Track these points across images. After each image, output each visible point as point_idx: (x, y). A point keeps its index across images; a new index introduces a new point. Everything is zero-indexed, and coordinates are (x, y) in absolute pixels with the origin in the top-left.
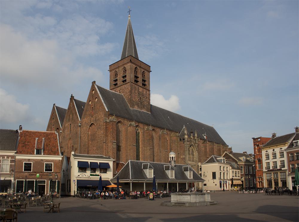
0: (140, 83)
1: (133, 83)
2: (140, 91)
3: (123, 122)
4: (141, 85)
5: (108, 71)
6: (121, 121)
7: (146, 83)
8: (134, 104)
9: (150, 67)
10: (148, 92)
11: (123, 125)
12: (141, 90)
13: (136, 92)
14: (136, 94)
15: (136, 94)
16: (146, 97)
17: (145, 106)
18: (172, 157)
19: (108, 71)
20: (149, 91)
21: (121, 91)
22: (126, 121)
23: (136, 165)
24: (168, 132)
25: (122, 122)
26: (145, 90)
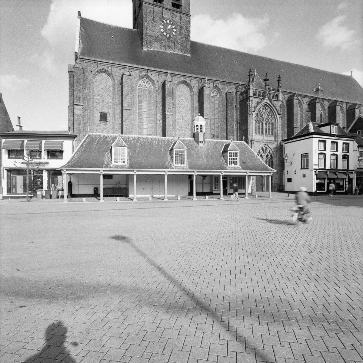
1: (150, 4)
3: (110, 71)
4: (170, 6)
6: (106, 68)
8: (150, 41)
11: (111, 76)
12: (167, 15)
13: (156, 19)
14: (156, 24)
15: (156, 24)
16: (181, 27)
18: (197, 126)
20: (188, 15)
22: (118, 69)
23: (98, 142)
24: (220, 86)
25: (108, 71)
26: (178, 15)
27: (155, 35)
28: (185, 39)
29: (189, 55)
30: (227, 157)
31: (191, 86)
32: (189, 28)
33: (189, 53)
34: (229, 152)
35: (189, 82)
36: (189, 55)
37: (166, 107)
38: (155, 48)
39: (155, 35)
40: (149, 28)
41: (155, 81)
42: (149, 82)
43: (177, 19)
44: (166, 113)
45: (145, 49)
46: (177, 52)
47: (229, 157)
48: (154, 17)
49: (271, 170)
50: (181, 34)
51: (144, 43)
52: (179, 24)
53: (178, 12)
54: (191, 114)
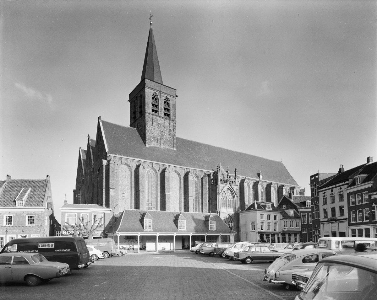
0: (161, 113)
2: (159, 122)
3: (129, 164)
4: (163, 115)
5: (128, 101)
6: (127, 162)
7: (171, 113)
9: (176, 90)
10: (172, 124)
12: (161, 121)
14: (153, 128)
16: (170, 130)
17: (169, 141)
19: (128, 101)
20: (174, 121)
21: (139, 125)
25: (128, 164)
26: (168, 121)
27: (153, 136)
28: (172, 138)
29: (175, 149)
30: (208, 224)
31: (179, 174)
32: (175, 131)
33: (175, 148)
34: (209, 221)
35: (178, 171)
36: (175, 149)
37: (166, 189)
38: (154, 144)
39: (153, 136)
40: (149, 131)
41: (157, 170)
42: (153, 171)
43: (167, 124)
44: (166, 193)
45: (147, 145)
46: (167, 147)
47: (209, 225)
48: (153, 123)
49: (235, 233)
50: (170, 134)
51: (147, 142)
52: (169, 127)
53: (168, 119)
54: (179, 193)
